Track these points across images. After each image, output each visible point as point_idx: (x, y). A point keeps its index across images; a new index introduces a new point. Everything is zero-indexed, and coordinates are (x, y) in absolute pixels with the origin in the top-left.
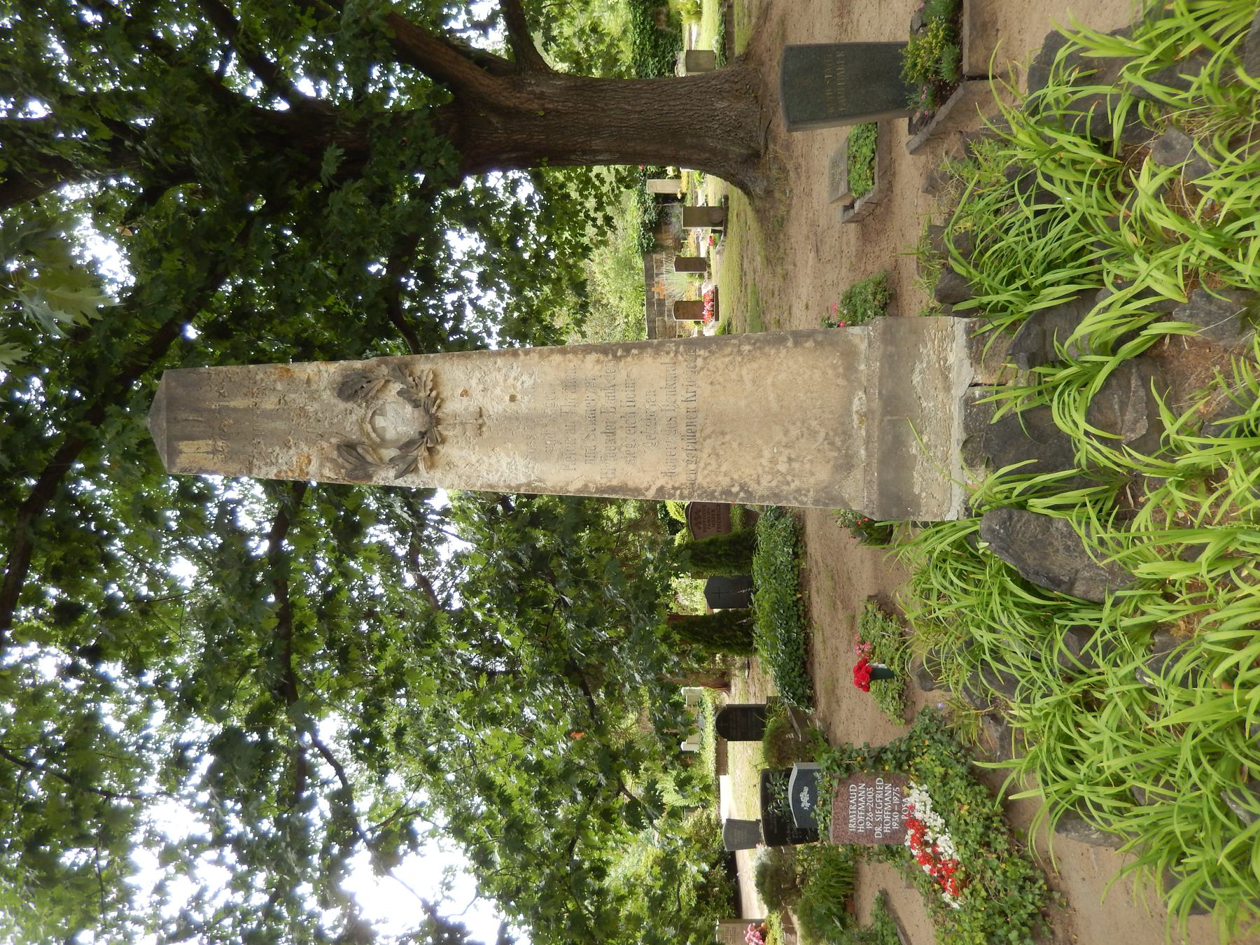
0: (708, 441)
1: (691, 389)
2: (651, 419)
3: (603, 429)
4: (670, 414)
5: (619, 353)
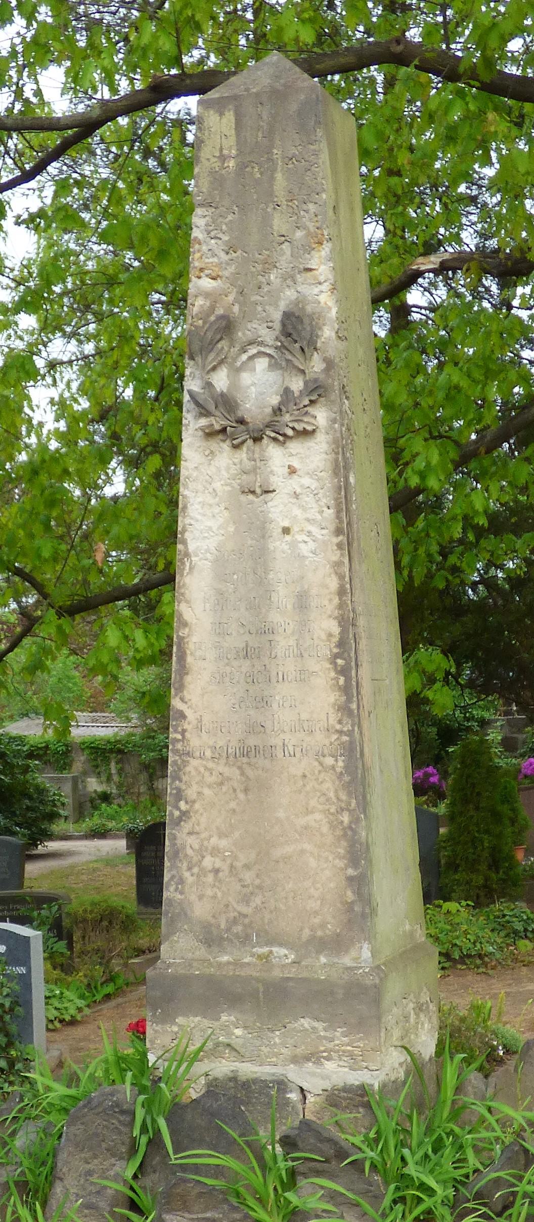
0: (238, 772)
1: (298, 750)
2: (263, 702)
3: (250, 644)
4: (268, 725)
5: (340, 662)
